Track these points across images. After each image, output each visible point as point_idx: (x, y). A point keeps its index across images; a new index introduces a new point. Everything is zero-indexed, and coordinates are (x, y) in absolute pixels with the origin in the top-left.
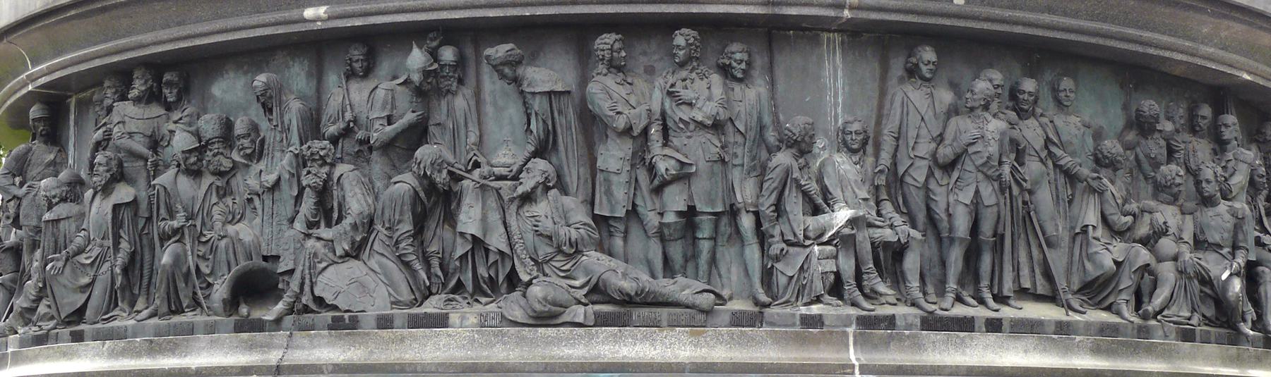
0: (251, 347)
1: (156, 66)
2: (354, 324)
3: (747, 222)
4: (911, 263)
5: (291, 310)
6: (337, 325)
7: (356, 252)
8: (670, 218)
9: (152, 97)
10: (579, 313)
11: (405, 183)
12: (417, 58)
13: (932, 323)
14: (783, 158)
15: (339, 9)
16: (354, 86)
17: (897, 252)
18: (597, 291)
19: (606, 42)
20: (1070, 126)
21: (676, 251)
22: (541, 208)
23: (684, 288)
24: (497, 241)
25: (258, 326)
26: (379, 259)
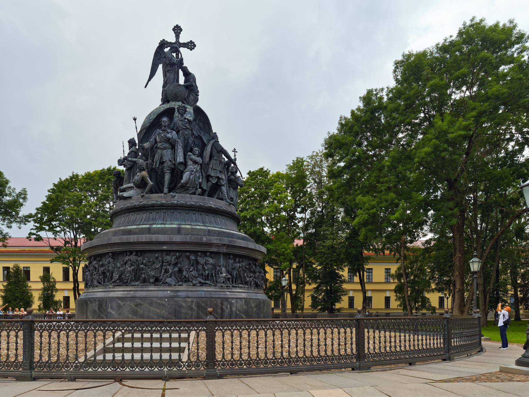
0: (158, 287)
1: (137, 251)
2: (171, 285)
3: (214, 275)
4: (231, 280)
5: (162, 283)
6: (169, 285)
7: (170, 277)
8: (206, 274)
9: (136, 255)
10: (198, 285)
11: (176, 269)
12: (178, 254)
13: (233, 287)
14: (218, 268)
16: (167, 256)
17: (229, 278)
18: (200, 282)
19: (199, 254)
20: (244, 264)
21: (206, 278)
22: (192, 273)
23: (207, 282)
24: (187, 276)
25: (158, 285)
26: (173, 277)
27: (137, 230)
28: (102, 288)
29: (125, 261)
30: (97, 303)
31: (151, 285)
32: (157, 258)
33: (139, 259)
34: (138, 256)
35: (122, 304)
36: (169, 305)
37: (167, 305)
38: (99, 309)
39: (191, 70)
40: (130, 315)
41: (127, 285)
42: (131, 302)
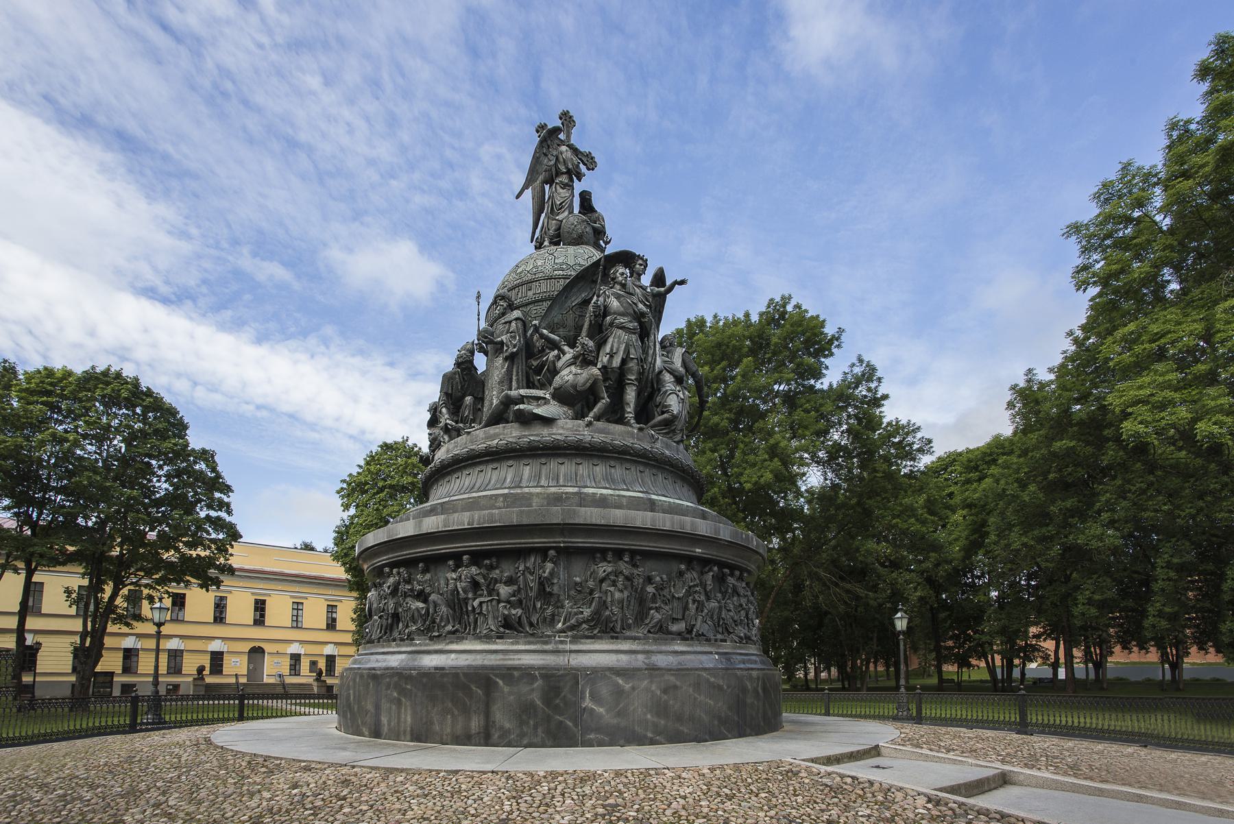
0: (689, 645)
1: (633, 553)
6: (706, 640)
15: (704, 551)
27: (624, 501)
28: (530, 643)
29: (601, 574)
30: (539, 683)
31: (673, 639)
32: (681, 574)
33: (635, 572)
34: (635, 566)
35: (627, 687)
36: (728, 687)
37: (725, 687)
38: (547, 701)
39: (597, 204)
40: (649, 716)
41: (617, 638)
42: (651, 682)
